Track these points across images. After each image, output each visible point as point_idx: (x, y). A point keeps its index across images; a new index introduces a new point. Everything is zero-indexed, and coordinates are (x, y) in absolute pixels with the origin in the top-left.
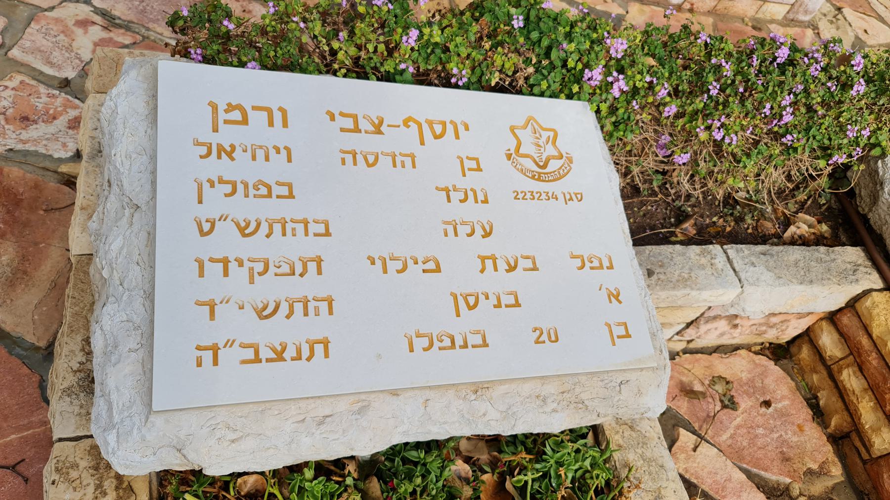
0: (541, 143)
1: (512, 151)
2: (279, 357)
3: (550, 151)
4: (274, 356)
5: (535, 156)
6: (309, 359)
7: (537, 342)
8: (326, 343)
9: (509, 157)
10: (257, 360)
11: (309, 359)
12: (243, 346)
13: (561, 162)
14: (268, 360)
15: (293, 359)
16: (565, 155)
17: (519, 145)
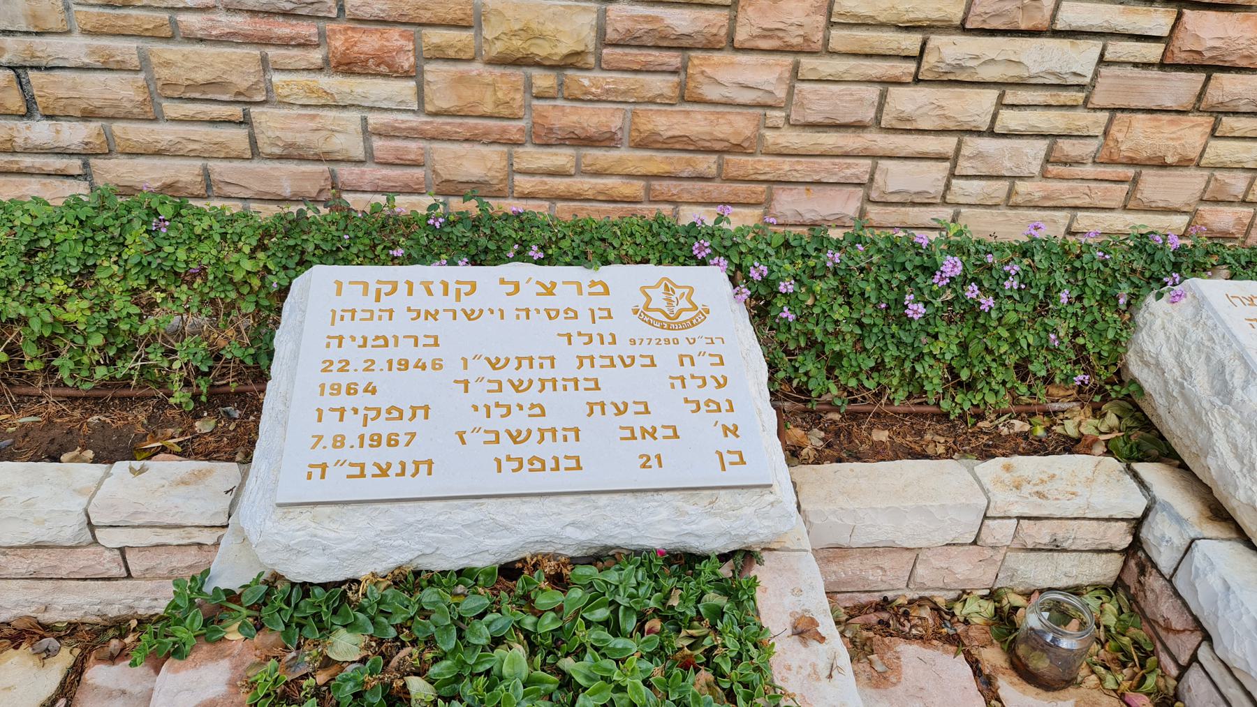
0: (673, 298)
1: (641, 308)
2: (384, 473)
3: (684, 303)
4: (378, 472)
5: (666, 310)
6: (413, 476)
7: (644, 466)
8: (430, 463)
9: (635, 312)
10: (362, 475)
11: (413, 476)
12: (351, 465)
13: (694, 313)
14: (374, 476)
15: (397, 475)
16: (700, 307)
17: (649, 299)
